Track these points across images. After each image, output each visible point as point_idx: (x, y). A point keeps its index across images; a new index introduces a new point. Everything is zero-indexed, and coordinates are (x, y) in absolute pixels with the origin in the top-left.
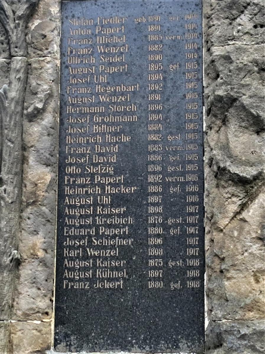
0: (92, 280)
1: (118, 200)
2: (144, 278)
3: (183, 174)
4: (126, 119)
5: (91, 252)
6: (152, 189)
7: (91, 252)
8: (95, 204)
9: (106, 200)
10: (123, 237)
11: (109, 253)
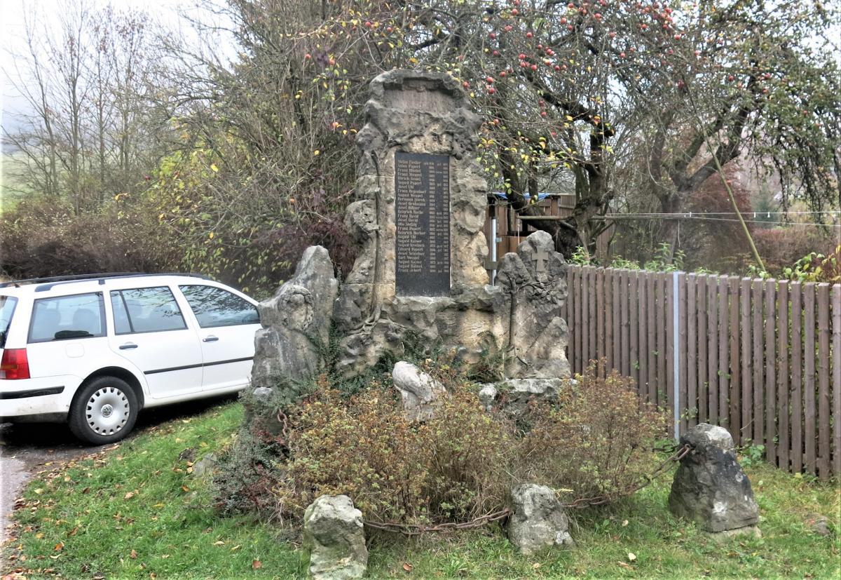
0: (409, 269)
1: (419, 237)
2: (429, 268)
3: (442, 228)
4: (421, 204)
5: (409, 258)
6: (431, 233)
7: (409, 258)
8: (410, 238)
9: (414, 237)
10: (421, 252)
11: (415, 258)
